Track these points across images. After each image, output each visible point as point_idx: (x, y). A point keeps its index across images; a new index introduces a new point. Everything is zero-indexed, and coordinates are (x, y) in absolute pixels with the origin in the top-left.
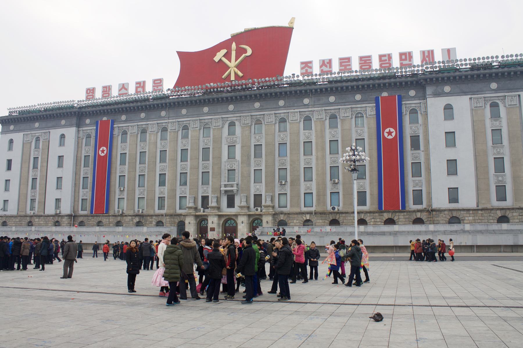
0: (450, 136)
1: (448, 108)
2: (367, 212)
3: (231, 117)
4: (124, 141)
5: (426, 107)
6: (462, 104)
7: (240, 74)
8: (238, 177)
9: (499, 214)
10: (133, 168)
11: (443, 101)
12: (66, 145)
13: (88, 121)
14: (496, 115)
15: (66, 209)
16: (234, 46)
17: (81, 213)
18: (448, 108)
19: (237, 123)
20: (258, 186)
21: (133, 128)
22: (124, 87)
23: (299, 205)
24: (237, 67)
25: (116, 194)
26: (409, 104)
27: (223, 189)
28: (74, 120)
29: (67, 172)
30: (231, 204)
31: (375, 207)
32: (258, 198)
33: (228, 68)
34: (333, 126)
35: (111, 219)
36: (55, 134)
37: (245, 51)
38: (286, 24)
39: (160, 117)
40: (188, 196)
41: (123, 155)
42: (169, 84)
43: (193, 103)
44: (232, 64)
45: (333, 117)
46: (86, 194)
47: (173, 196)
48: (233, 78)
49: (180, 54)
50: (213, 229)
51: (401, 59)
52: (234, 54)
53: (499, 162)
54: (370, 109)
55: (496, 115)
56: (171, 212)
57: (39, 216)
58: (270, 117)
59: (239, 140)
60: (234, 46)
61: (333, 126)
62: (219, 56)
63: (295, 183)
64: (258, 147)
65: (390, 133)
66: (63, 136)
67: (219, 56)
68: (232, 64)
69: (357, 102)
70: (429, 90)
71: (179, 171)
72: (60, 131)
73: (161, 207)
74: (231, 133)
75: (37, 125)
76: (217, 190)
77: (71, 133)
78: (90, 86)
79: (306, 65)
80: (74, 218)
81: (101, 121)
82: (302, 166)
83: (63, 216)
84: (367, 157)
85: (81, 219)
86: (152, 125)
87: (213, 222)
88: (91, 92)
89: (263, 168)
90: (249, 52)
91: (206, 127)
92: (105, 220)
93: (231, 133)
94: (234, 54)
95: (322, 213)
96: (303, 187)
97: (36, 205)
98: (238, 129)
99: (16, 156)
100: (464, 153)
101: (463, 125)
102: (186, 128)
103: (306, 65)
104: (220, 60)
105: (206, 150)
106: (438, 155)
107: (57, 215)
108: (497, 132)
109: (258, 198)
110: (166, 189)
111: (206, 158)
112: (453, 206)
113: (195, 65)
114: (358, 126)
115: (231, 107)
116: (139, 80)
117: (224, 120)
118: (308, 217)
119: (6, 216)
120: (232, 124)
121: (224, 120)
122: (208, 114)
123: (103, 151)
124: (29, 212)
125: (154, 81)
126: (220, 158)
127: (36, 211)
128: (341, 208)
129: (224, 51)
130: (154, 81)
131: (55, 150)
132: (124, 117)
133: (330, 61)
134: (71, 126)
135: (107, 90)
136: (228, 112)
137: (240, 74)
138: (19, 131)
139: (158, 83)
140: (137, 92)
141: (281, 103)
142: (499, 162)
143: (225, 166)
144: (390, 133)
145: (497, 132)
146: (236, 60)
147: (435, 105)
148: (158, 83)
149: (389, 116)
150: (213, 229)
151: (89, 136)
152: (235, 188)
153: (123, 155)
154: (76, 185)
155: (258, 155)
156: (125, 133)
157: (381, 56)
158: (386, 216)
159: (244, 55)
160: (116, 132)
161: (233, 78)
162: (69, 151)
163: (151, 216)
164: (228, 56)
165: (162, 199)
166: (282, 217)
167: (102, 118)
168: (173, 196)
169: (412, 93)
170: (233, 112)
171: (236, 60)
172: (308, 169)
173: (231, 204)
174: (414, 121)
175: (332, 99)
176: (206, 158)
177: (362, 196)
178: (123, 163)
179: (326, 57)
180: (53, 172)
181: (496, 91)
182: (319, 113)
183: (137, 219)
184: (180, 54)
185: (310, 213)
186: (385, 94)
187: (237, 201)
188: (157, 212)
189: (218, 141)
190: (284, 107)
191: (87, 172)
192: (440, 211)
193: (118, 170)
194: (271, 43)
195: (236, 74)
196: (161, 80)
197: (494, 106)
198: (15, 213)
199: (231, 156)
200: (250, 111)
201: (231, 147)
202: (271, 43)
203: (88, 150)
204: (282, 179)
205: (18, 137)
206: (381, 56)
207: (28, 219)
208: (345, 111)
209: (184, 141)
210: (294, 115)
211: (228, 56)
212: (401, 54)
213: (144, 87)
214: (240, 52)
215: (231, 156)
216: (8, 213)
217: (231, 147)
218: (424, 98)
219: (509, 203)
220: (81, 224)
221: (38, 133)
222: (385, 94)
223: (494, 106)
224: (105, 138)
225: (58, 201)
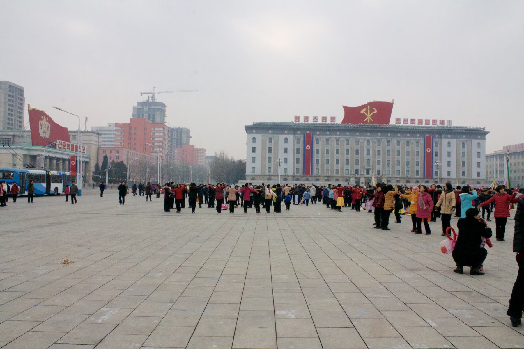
0: (449, 154)
1: (449, 143)
2: (419, 178)
3: (368, 138)
4: (318, 143)
5: (441, 142)
6: (453, 141)
8: (371, 162)
9: (462, 180)
10: (323, 156)
11: (447, 140)
12: (291, 143)
13: (299, 132)
14: (463, 146)
15: (290, 172)
16: (369, 107)
17: (296, 174)
18: (449, 143)
19: (371, 141)
20: (379, 166)
21: (323, 138)
22: (315, 118)
23: (394, 174)
24: (371, 117)
25: (315, 166)
26: (435, 140)
27: (366, 167)
28: (293, 132)
29: (290, 156)
30: (368, 173)
31: (422, 176)
32: (379, 172)
33: (366, 117)
34: (408, 145)
35: (313, 178)
36: (282, 137)
37: (374, 111)
38: (391, 102)
39: (336, 135)
40: (348, 170)
43: (352, 131)
44: (369, 115)
45: (408, 142)
46: (300, 166)
47: (342, 169)
48: (369, 122)
49: (345, 108)
50: (362, 183)
51: (433, 122)
52: (369, 111)
53: (463, 163)
54: (422, 141)
55: (463, 146)
56: (342, 175)
57: (274, 176)
58: (384, 140)
59: (371, 148)
60: (369, 107)
61: (408, 145)
62: (363, 111)
63: (393, 167)
64: (379, 151)
65: (428, 150)
66: (286, 139)
67: (363, 111)
68: (369, 115)
69: (417, 137)
70: (443, 136)
71: (345, 158)
72: (285, 136)
73: (337, 173)
74: (368, 144)
75: (270, 131)
76: (362, 167)
77: (291, 138)
78: (297, 115)
79: (398, 120)
80: (294, 176)
81: (307, 134)
82: (396, 160)
83: (289, 176)
84: (421, 158)
85: (296, 178)
86: (333, 138)
87: (362, 180)
88: (297, 118)
89: (381, 159)
90: (376, 111)
91: (357, 142)
92: (310, 178)
93: (368, 144)
94: (369, 111)
95: (404, 178)
96: (396, 168)
97: (272, 170)
98: (371, 143)
99: (258, 146)
100: (453, 159)
101: (453, 150)
102: (348, 140)
103: (398, 120)
104: (364, 113)
106: (445, 159)
107: (286, 175)
108: (463, 153)
109: (379, 172)
110: (339, 166)
112: (449, 177)
113: (352, 114)
114: (417, 146)
115: (369, 134)
116: (323, 116)
117: (365, 139)
118: (398, 179)
119: (255, 175)
120: (368, 141)
121: (365, 139)
122: (358, 136)
123: (308, 147)
124: (267, 173)
125: (331, 118)
126: (363, 154)
127: (272, 173)
128: (409, 176)
129: (365, 110)
130: (331, 118)
131: (282, 145)
132: (318, 133)
133: (407, 120)
134: (291, 134)
135: (306, 119)
136: (367, 136)
138: (259, 133)
139: (333, 119)
140: (322, 121)
141: (389, 134)
142: (463, 163)
143: (366, 157)
144: (428, 150)
145: (463, 153)
146: (371, 113)
147: (445, 141)
148: (333, 119)
149: (428, 143)
150: (362, 183)
151: (298, 139)
152: (371, 167)
154: (294, 162)
155: (379, 154)
156: (318, 140)
157: (426, 120)
158: (426, 180)
160: (314, 139)
161: (369, 122)
162: (290, 146)
163: (333, 177)
164: (366, 111)
165: (337, 170)
166: (389, 179)
167: (308, 133)
168: (342, 169)
169: (437, 136)
170: (370, 136)
171: (371, 113)
172: (398, 161)
173: (368, 173)
174: (436, 146)
175: (408, 135)
177: (417, 172)
179: (406, 118)
180: (281, 156)
181: (465, 138)
182: (403, 141)
183: (326, 178)
184: (345, 108)
185: (400, 178)
186: (427, 135)
187: (371, 171)
188: (335, 175)
189: (362, 147)
190: (390, 136)
191: (301, 156)
192: (445, 179)
193: (315, 156)
194: (384, 109)
195: (370, 120)
196: (334, 118)
197: (463, 143)
198: (260, 174)
199: (368, 153)
200: (376, 136)
201: (368, 151)
202: (384, 109)
203: (301, 146)
204: (388, 164)
205: (259, 137)
206: (426, 120)
207: (268, 177)
208: (413, 141)
209: (347, 146)
210: (394, 140)
211: (366, 111)
212: (433, 120)
213: (326, 119)
214: (371, 111)
215: (368, 153)
216: (256, 173)
217: (368, 151)
218: (441, 138)
219: (465, 177)
220: (298, 180)
221: (270, 136)
222: (427, 135)
223: (463, 143)
224: (308, 140)
225: (285, 169)
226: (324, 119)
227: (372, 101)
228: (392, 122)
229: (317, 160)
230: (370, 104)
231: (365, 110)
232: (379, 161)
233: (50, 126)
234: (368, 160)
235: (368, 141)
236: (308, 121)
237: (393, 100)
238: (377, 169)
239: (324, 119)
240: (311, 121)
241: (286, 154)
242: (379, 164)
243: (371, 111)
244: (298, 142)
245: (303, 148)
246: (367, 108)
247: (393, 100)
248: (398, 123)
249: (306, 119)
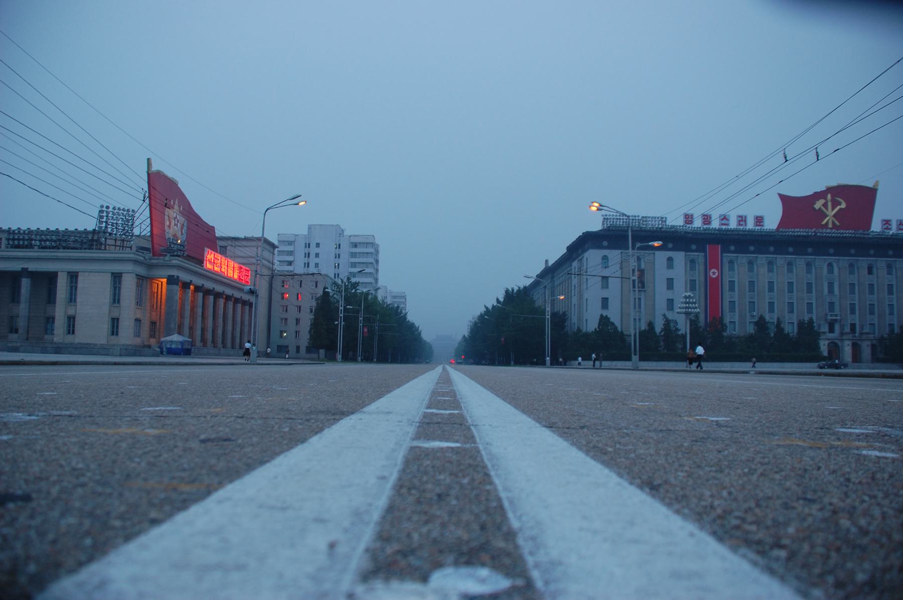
4: (731, 269)
7: (838, 223)
8: (837, 307)
16: (829, 196)
19: (835, 264)
21: (743, 259)
24: (834, 216)
27: (829, 317)
30: (831, 330)
37: (840, 204)
38: (870, 184)
41: (732, 283)
42: (772, 223)
48: (830, 226)
49: (783, 198)
52: (830, 204)
60: (829, 196)
62: (818, 205)
67: (818, 205)
68: (831, 213)
77: (679, 257)
79: (887, 222)
82: (887, 303)
88: (689, 218)
89: (856, 302)
90: (843, 206)
94: (830, 204)
104: (820, 209)
105: (809, 285)
109: (853, 326)
111: (809, 291)
116: (741, 214)
129: (822, 201)
135: (707, 219)
137: (838, 223)
139: (759, 220)
146: (833, 209)
148: (759, 220)
151: (692, 262)
153: (732, 283)
155: (852, 292)
159: (838, 207)
160: (724, 261)
161: (830, 226)
164: (825, 205)
173: (831, 330)
176: (809, 291)
178: (732, 289)
184: (783, 198)
187: (837, 327)
195: (833, 223)
199: (831, 291)
201: (831, 285)
202: (860, 199)
211: (825, 205)
214: (835, 204)
215: (831, 291)
217: (831, 285)
226: (742, 219)
227: (834, 183)
228: (876, 226)
229: (732, 303)
230: (830, 190)
231: (822, 201)
232: (853, 307)
233: (185, 224)
234: (832, 304)
235: (830, 265)
236: (709, 223)
237: (877, 183)
238: (849, 322)
239: (742, 219)
240: (715, 224)
241: (670, 292)
242: (853, 312)
243: (835, 204)
244: (693, 268)
245: (702, 279)
246: (826, 199)
247: (877, 183)
248: (887, 228)
249: (707, 219)
